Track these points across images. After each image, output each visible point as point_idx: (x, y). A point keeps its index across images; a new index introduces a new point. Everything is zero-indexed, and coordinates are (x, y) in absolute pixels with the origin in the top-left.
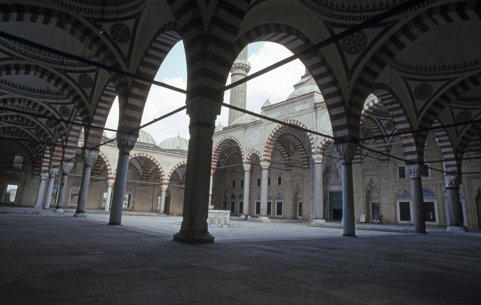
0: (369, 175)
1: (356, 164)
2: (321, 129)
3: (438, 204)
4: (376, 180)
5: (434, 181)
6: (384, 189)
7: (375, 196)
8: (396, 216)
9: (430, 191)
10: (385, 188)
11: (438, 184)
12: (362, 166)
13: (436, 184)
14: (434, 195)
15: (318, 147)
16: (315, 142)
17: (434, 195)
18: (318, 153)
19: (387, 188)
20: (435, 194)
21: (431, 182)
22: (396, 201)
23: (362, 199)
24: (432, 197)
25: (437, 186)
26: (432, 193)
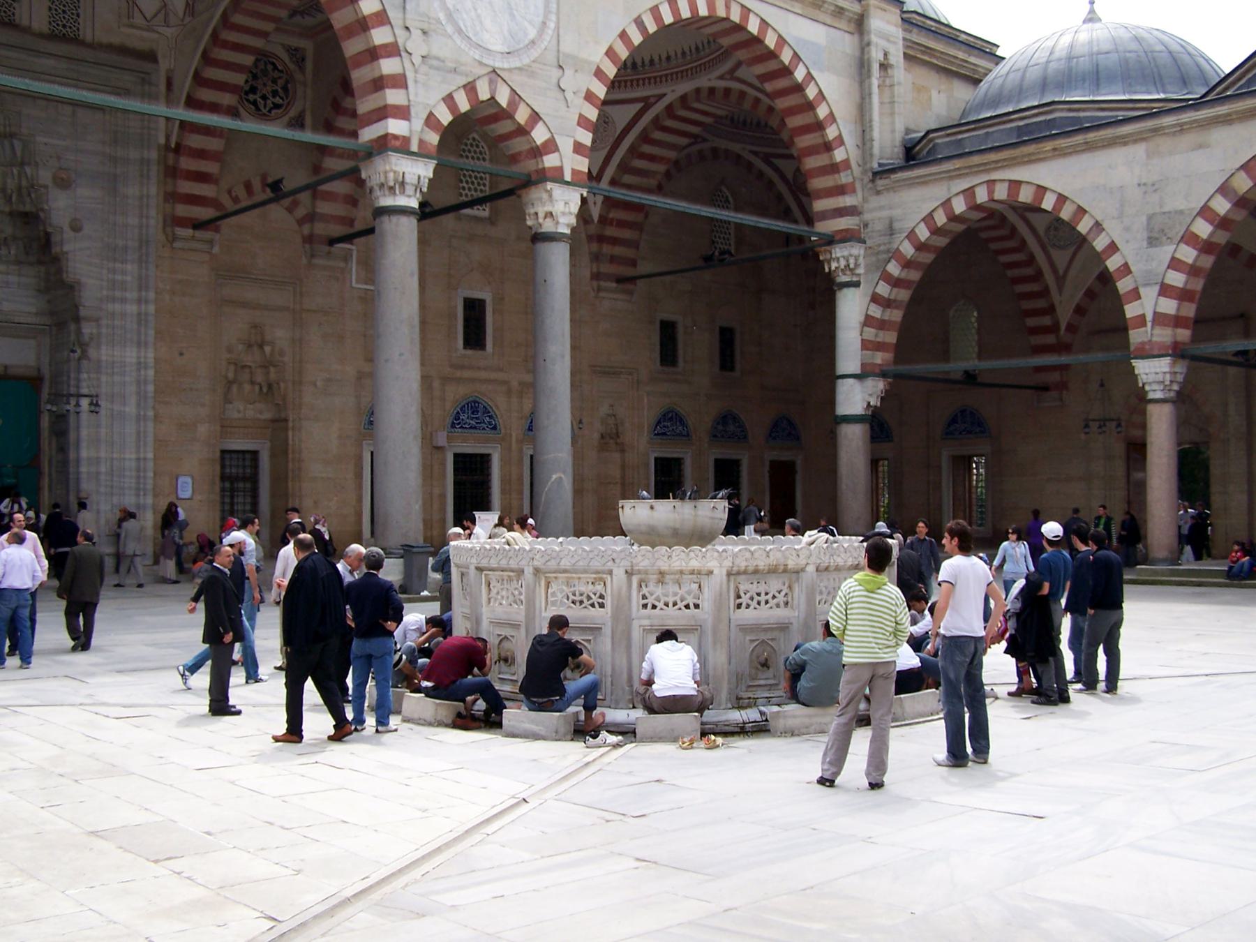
0: (244, 305)
1: (190, 232)
2: (450, 16)
3: (505, 462)
4: (280, 335)
5: (501, 370)
6: (315, 385)
7: (236, 415)
8: (359, 515)
9: (486, 411)
10: (318, 383)
11: (515, 384)
12: (216, 250)
13: (505, 382)
14: (495, 428)
15: (431, 121)
16: (410, 76)
17: (495, 428)
18: (423, 154)
19: (329, 380)
20: (501, 422)
21: (493, 376)
22: (361, 445)
23: (203, 429)
24: (491, 434)
25: (509, 393)
26: (491, 417)
